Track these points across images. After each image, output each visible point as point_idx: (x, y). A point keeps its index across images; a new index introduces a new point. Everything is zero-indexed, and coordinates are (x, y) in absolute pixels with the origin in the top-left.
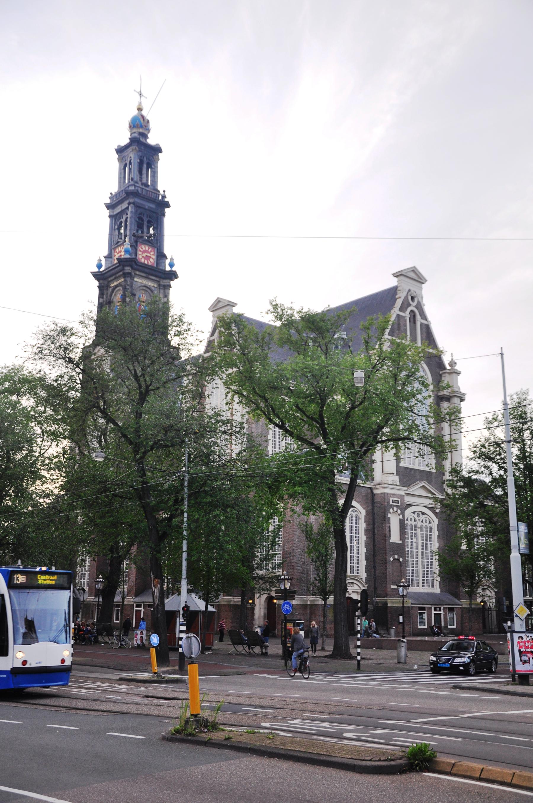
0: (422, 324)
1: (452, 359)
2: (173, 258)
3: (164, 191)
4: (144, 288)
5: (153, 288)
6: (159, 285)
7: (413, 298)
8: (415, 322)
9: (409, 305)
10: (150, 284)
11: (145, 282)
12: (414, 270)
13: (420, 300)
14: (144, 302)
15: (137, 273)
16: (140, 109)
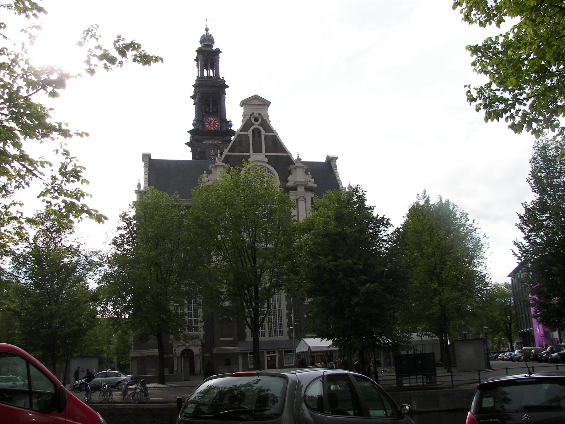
0: (266, 137)
1: (298, 157)
2: (231, 120)
3: (223, 78)
4: (212, 146)
5: (219, 145)
6: (223, 141)
7: (256, 120)
8: (260, 136)
9: (254, 124)
10: (216, 142)
11: (212, 142)
12: (256, 97)
13: (265, 118)
14: (213, 155)
15: (205, 137)
16: (207, 30)
